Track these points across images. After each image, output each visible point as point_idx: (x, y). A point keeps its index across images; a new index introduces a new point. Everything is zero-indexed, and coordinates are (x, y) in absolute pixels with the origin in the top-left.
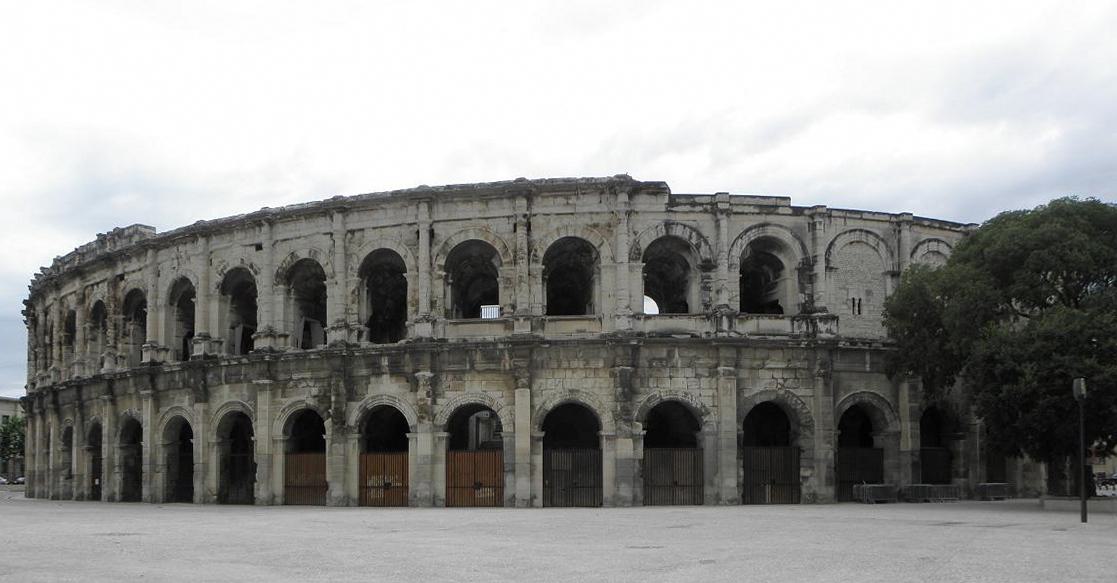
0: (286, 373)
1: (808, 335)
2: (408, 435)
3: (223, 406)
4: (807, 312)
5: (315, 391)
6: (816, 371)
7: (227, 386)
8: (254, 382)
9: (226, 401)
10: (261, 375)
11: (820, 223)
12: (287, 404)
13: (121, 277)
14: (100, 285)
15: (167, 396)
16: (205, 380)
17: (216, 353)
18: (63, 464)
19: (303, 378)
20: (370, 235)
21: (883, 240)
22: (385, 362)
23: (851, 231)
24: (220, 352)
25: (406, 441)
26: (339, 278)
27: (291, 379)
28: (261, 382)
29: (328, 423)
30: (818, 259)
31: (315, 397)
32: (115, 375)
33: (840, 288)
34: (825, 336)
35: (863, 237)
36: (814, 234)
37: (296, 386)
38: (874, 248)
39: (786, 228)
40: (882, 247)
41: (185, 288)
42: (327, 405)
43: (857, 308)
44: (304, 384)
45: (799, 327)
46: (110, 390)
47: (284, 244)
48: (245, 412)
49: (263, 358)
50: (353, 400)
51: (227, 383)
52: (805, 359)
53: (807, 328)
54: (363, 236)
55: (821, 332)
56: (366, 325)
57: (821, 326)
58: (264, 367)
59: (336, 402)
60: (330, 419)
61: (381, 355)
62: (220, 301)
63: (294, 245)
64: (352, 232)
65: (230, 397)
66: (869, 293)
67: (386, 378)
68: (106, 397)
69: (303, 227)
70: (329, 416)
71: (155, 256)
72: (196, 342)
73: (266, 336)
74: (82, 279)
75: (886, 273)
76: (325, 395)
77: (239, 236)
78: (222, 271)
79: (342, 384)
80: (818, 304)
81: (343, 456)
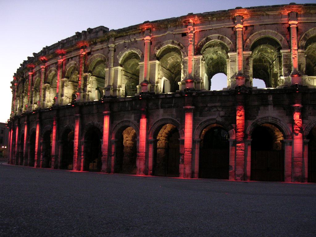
5: (222, 113)
9: (161, 118)
12: (203, 120)
14: (73, 58)
16: (147, 105)
18: (43, 149)
19: (215, 107)
22: (271, 98)
27: (207, 106)
31: (222, 117)
32: (85, 103)
37: (209, 110)
46: (80, 112)
51: (161, 108)
54: (253, 29)
61: (268, 94)
67: (270, 108)
68: (78, 115)
81: (240, 153)
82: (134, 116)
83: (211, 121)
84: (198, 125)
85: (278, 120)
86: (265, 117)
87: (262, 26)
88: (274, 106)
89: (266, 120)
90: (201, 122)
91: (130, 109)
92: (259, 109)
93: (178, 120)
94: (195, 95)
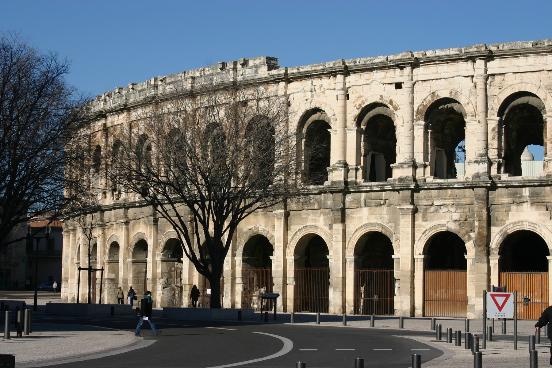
0: (427, 200)
2: (548, 257)
3: (361, 227)
5: (456, 216)
7: (367, 209)
8: (398, 207)
9: (365, 222)
10: (404, 200)
12: (427, 227)
13: (245, 103)
15: (300, 215)
16: (344, 203)
17: (353, 179)
18: (162, 273)
20: (509, 78)
24: (356, 177)
25: (547, 262)
26: (481, 117)
27: (432, 205)
28: (405, 207)
29: (469, 245)
31: (456, 221)
37: (436, 211)
41: (314, 117)
42: (467, 229)
44: (444, 209)
47: (424, 83)
48: (384, 232)
49: (408, 185)
50: (495, 225)
51: (365, 206)
56: (503, 158)
58: (408, 193)
59: (479, 228)
60: (471, 242)
62: (359, 132)
63: (434, 86)
64: (493, 75)
65: (368, 219)
67: (526, 206)
69: (445, 69)
70: (470, 238)
71: (286, 88)
72: (335, 168)
73: (409, 166)
74: (193, 101)
76: (466, 220)
77: (378, 75)
78: (360, 105)
79: (484, 211)
82: (325, 219)
83: (440, 228)
84: (421, 234)
85: (537, 227)
86: (519, 222)
87: (517, 75)
88: (532, 204)
89: (520, 227)
90: (425, 229)
91: (316, 206)
92: (510, 210)
93: (391, 227)
94: (413, 187)
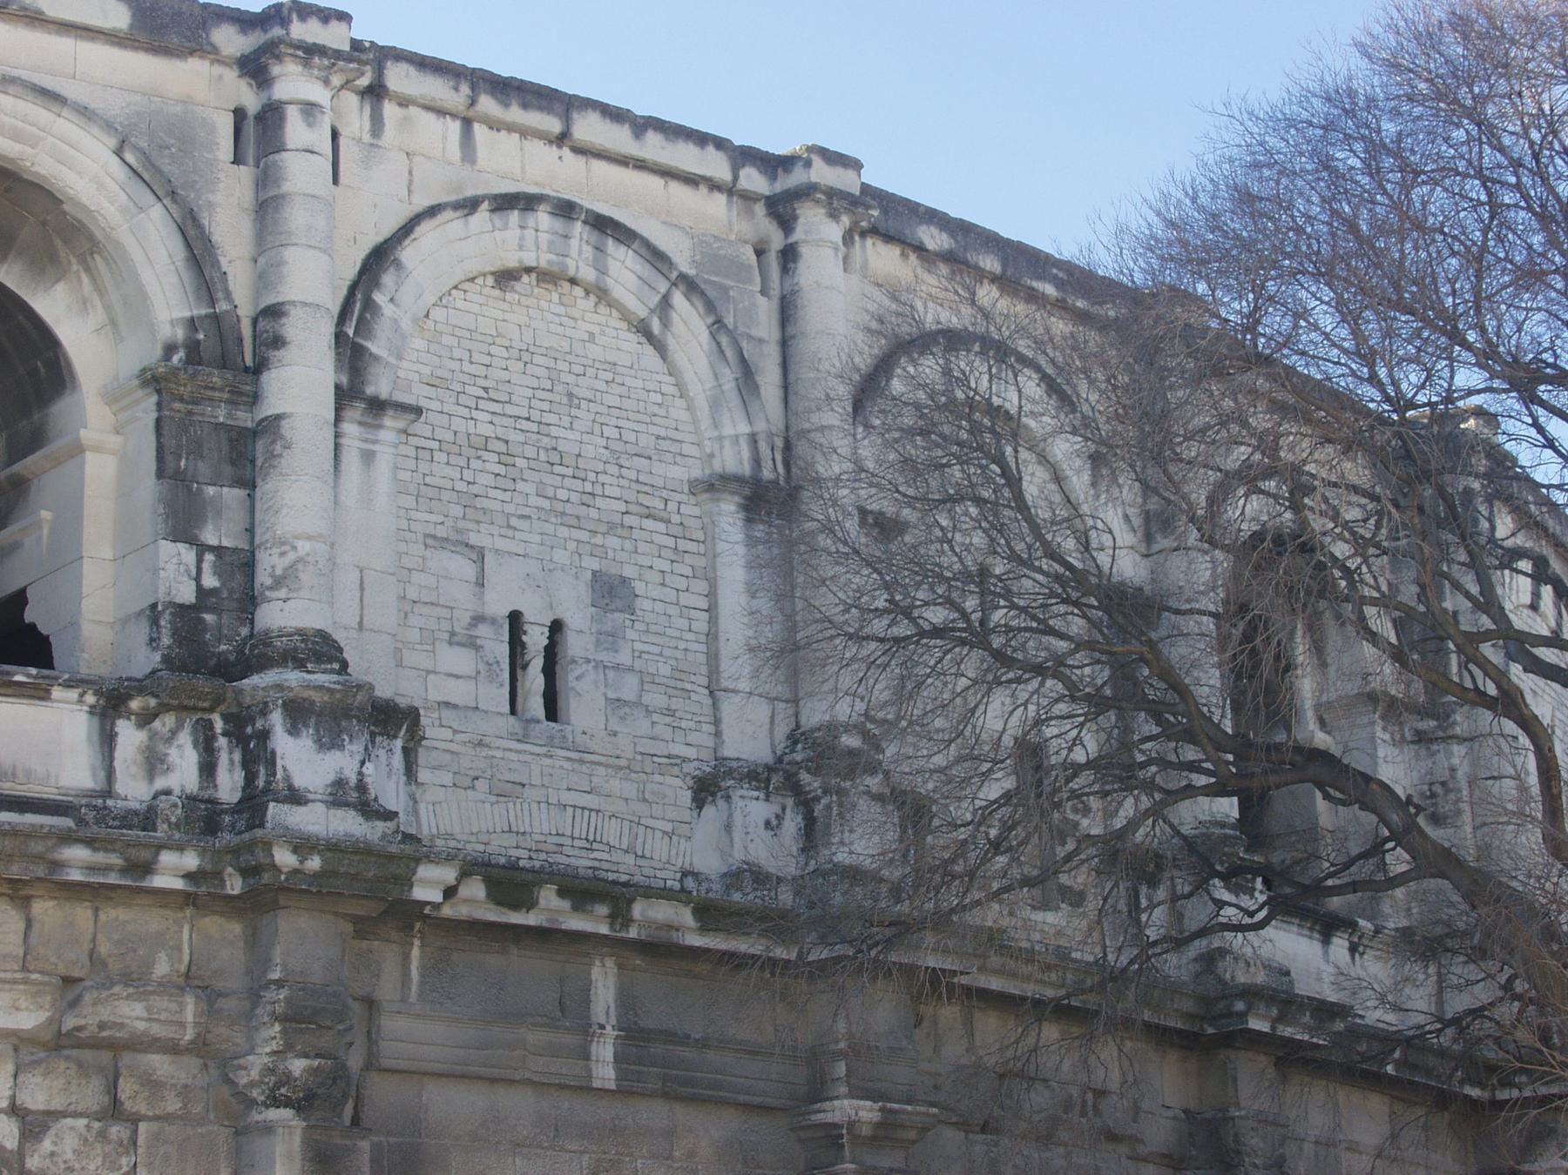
1: (203, 817)
4: (212, 660)
6: (255, 1065)
11: (310, 109)
21: (690, 286)
23: (506, 203)
30: (293, 327)
33: (434, 541)
34: (314, 820)
35: (579, 246)
36: (266, 179)
38: (643, 330)
39: (85, 113)
40: (689, 326)
43: (534, 679)
45: (154, 762)
52: (190, 980)
53: (208, 769)
55: (296, 797)
57: (301, 759)
66: (611, 592)
75: (714, 485)
80: (282, 615)
